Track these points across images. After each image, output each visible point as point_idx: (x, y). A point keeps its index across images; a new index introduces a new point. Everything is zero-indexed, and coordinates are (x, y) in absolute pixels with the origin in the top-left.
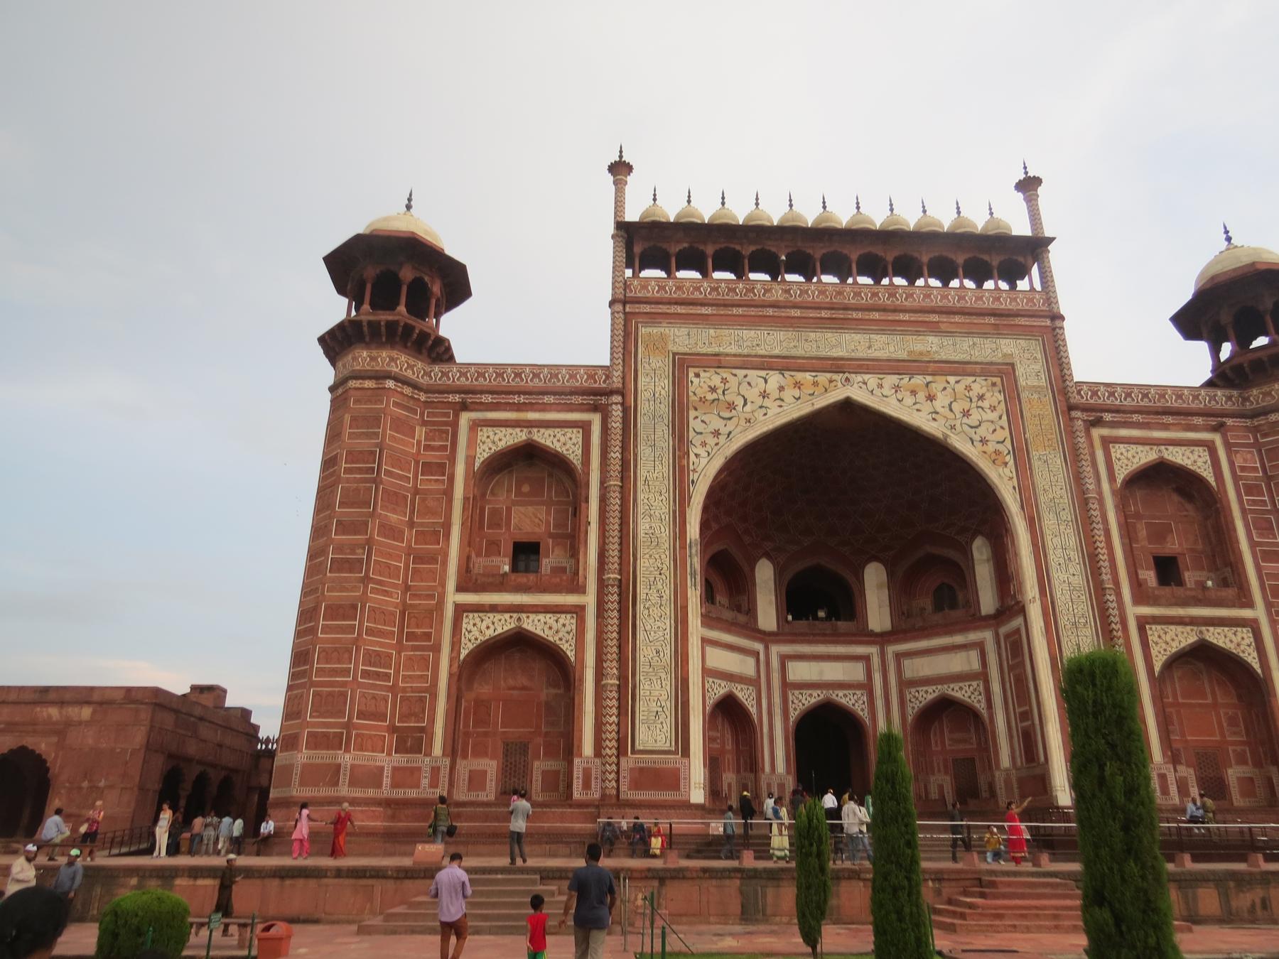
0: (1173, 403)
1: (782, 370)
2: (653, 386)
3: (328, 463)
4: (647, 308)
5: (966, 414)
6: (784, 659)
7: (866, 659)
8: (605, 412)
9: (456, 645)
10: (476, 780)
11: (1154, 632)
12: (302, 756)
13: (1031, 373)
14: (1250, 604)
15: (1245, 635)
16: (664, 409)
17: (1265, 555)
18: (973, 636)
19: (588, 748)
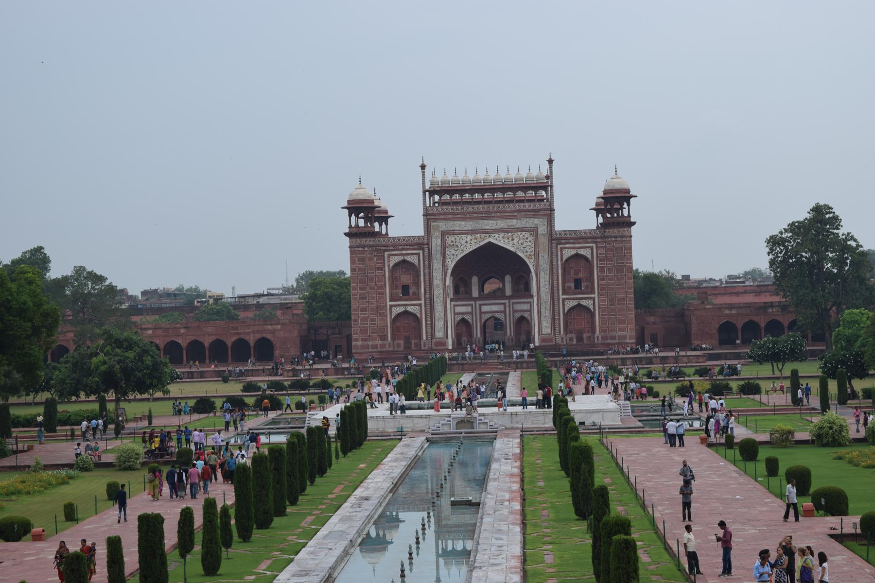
0: (584, 235)
1: (471, 234)
2: (436, 242)
4: (433, 217)
5: (522, 244)
6: (480, 305)
7: (505, 304)
8: (423, 250)
9: (391, 315)
10: (399, 345)
11: (566, 302)
12: (359, 343)
14: (594, 293)
15: (591, 301)
16: (439, 248)
17: (600, 279)
18: (529, 300)
19: (424, 338)
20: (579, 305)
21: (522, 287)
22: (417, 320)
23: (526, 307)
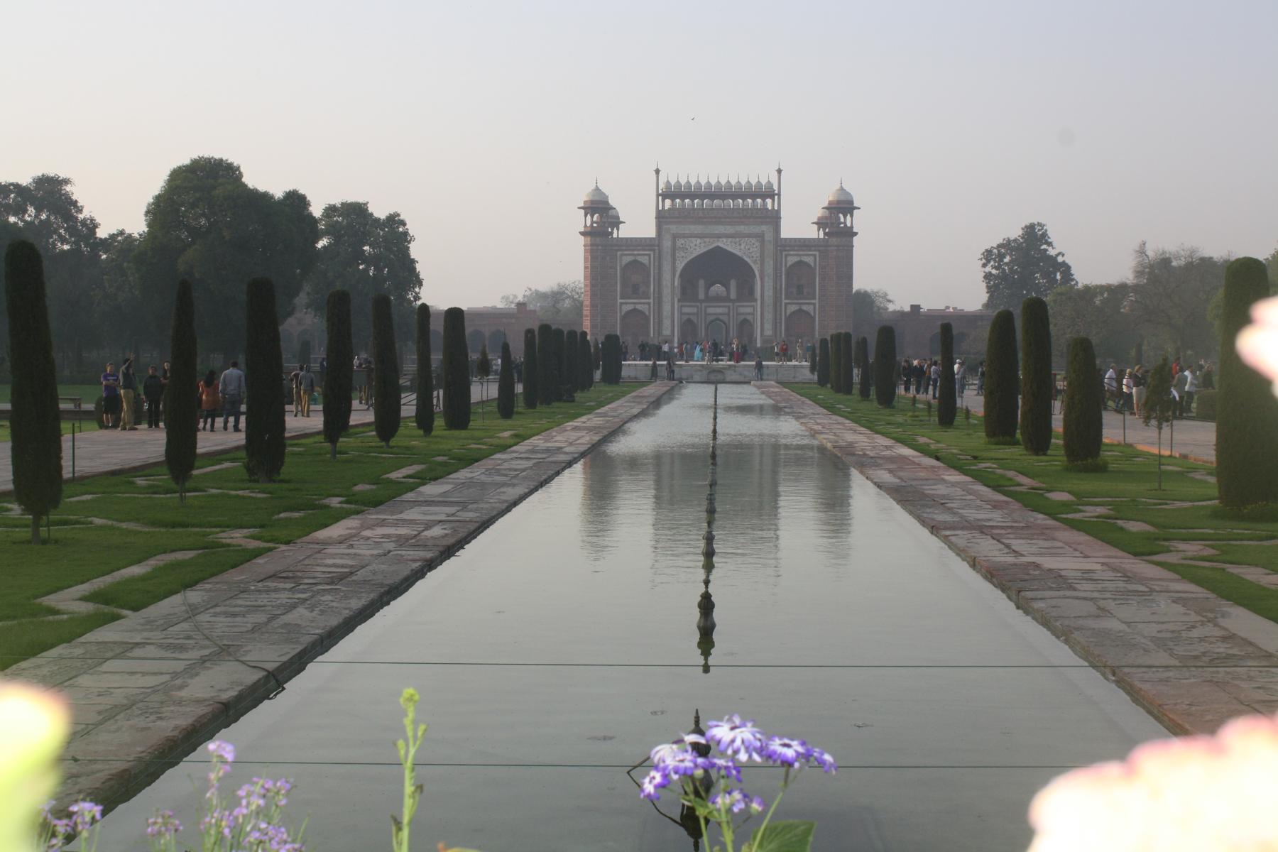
2: (667, 244)
3: (586, 268)
13: (769, 236)
20: (800, 310)
21: (746, 292)
22: (647, 318)
23: (749, 310)
